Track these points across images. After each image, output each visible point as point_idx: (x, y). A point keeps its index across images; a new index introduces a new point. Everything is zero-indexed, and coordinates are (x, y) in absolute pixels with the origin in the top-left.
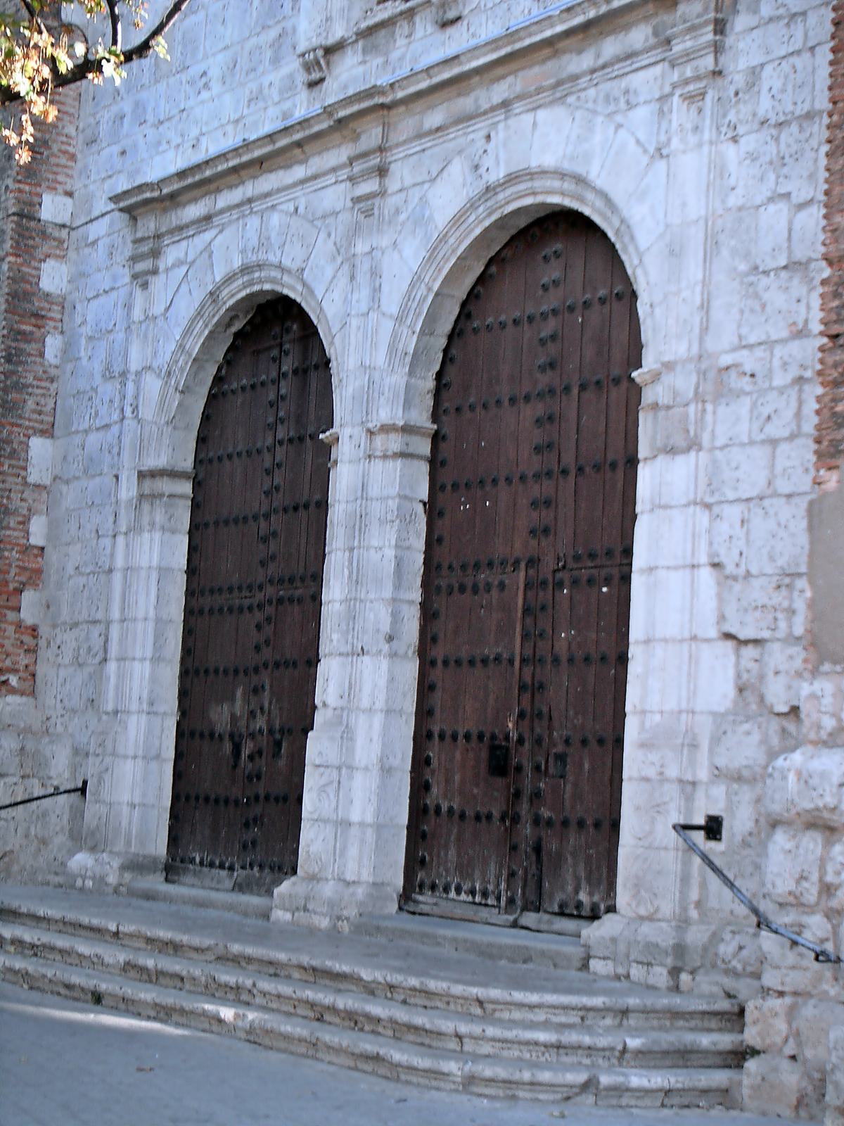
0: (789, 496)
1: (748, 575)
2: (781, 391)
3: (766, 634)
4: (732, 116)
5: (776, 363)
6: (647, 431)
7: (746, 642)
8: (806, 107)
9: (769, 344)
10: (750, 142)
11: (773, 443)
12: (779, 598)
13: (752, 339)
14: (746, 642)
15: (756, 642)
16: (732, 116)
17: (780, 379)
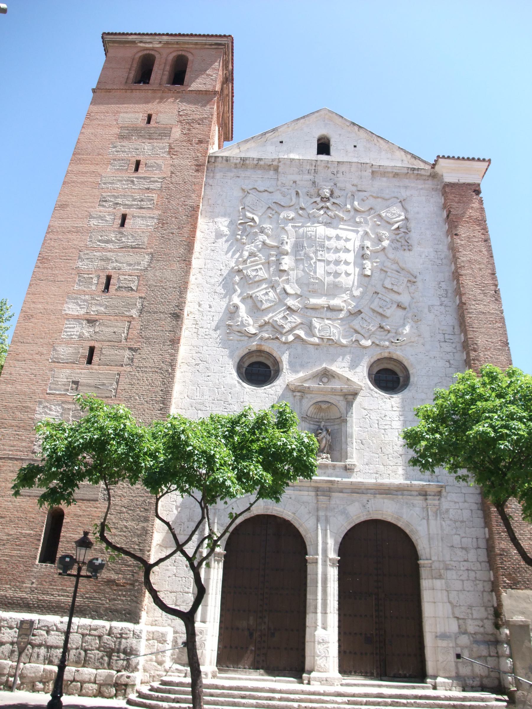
0: (468, 591)
1: (460, 606)
2: (464, 571)
3: (466, 617)
4: (443, 516)
5: (461, 565)
6: (424, 573)
7: (461, 619)
8: (461, 519)
9: (460, 562)
10: (448, 522)
11: (463, 581)
12: (469, 611)
13: (455, 560)
14: (461, 619)
15: (463, 619)
16: (443, 516)
17: (462, 568)
